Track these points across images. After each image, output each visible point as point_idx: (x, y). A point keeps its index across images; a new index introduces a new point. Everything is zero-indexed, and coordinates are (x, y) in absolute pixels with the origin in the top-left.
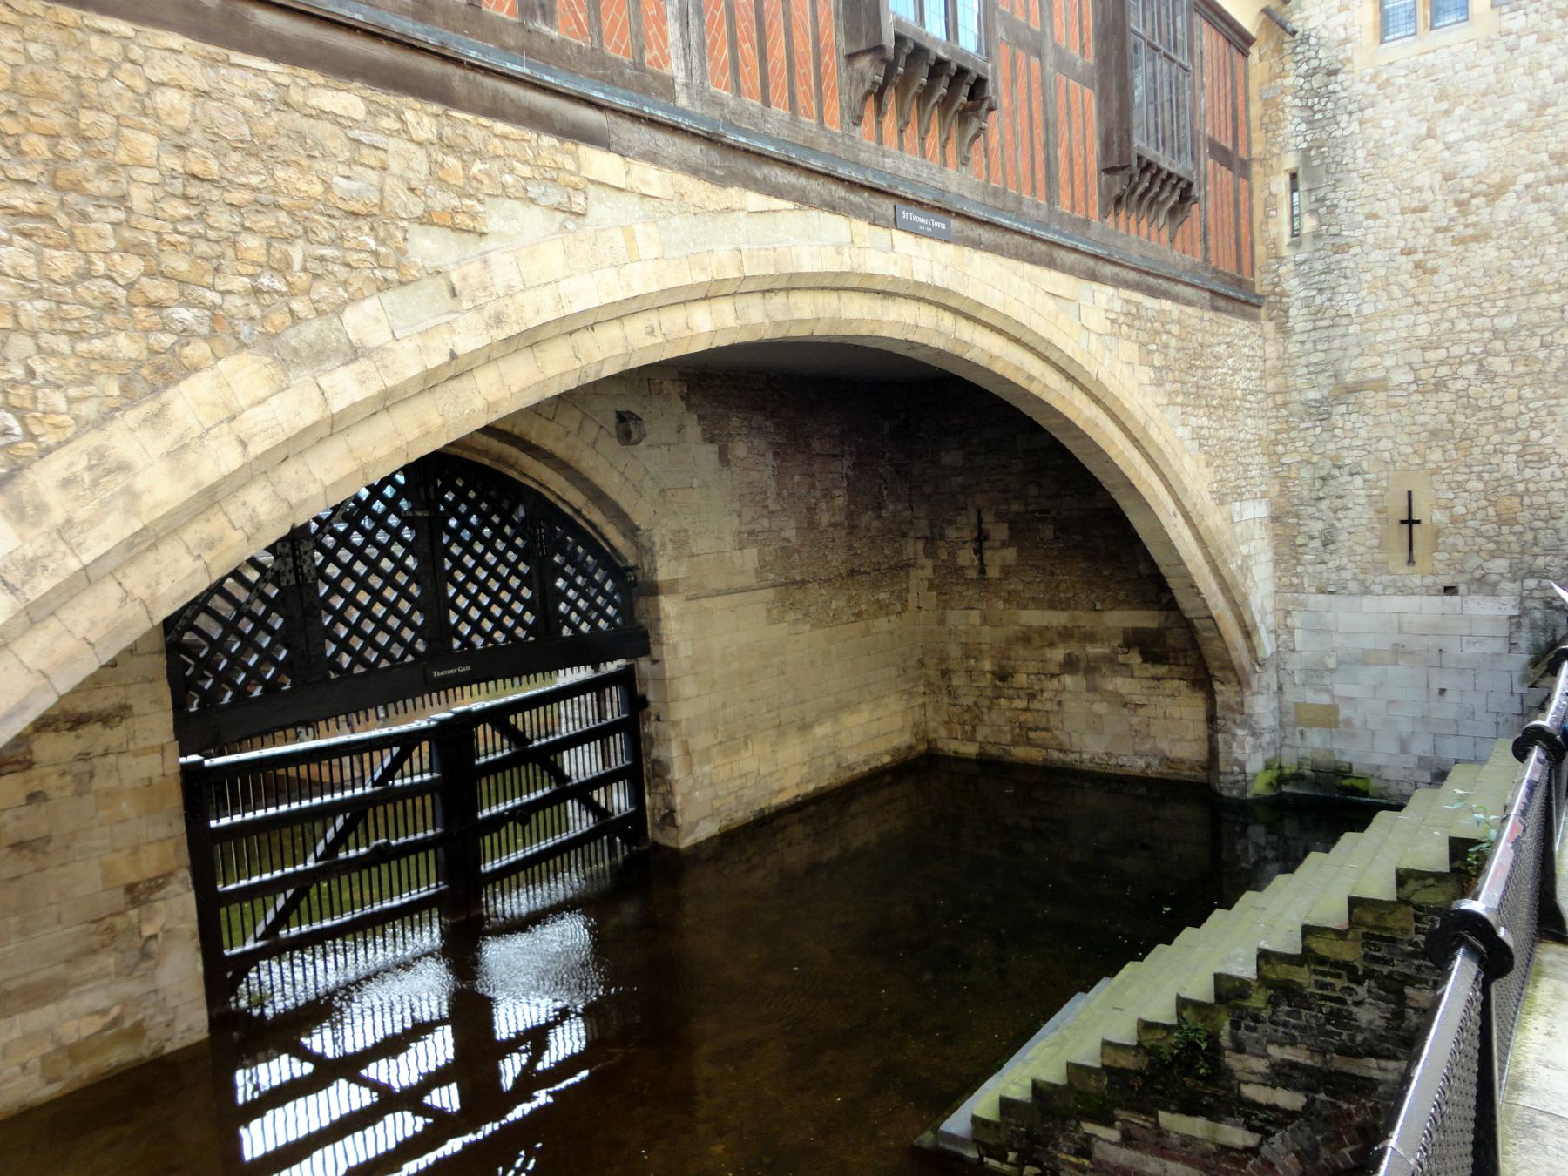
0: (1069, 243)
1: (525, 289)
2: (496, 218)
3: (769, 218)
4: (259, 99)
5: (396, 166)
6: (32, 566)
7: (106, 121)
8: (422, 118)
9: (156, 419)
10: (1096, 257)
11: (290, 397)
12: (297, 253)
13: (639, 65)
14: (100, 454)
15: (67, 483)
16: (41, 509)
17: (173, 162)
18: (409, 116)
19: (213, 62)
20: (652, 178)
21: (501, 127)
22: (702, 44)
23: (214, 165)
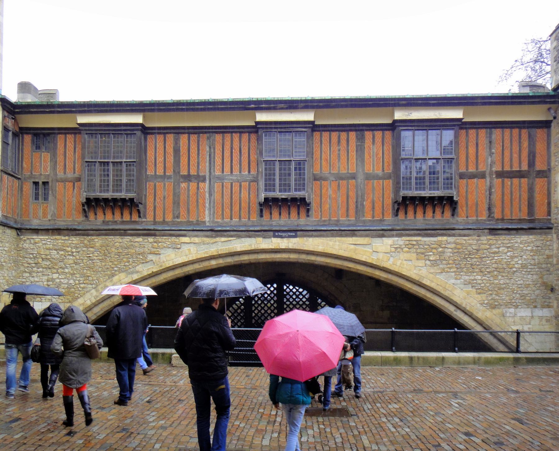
0: (363, 228)
1: (167, 261)
2: (162, 251)
3: (229, 242)
4: (127, 241)
5: (146, 246)
6: (97, 296)
7: (109, 248)
8: (151, 239)
9: (111, 281)
10: (383, 230)
11: (128, 278)
12: (131, 260)
13: (198, 221)
14: (105, 285)
15: (102, 288)
16: (99, 291)
17: (116, 251)
18: (149, 239)
19: (122, 238)
20: (196, 240)
21: (164, 238)
22: (214, 212)
23: (121, 251)
